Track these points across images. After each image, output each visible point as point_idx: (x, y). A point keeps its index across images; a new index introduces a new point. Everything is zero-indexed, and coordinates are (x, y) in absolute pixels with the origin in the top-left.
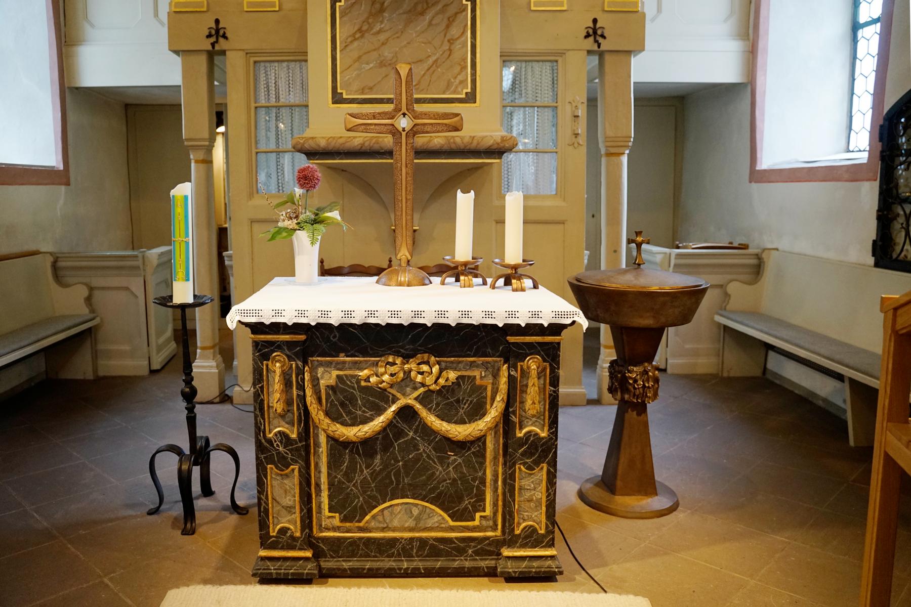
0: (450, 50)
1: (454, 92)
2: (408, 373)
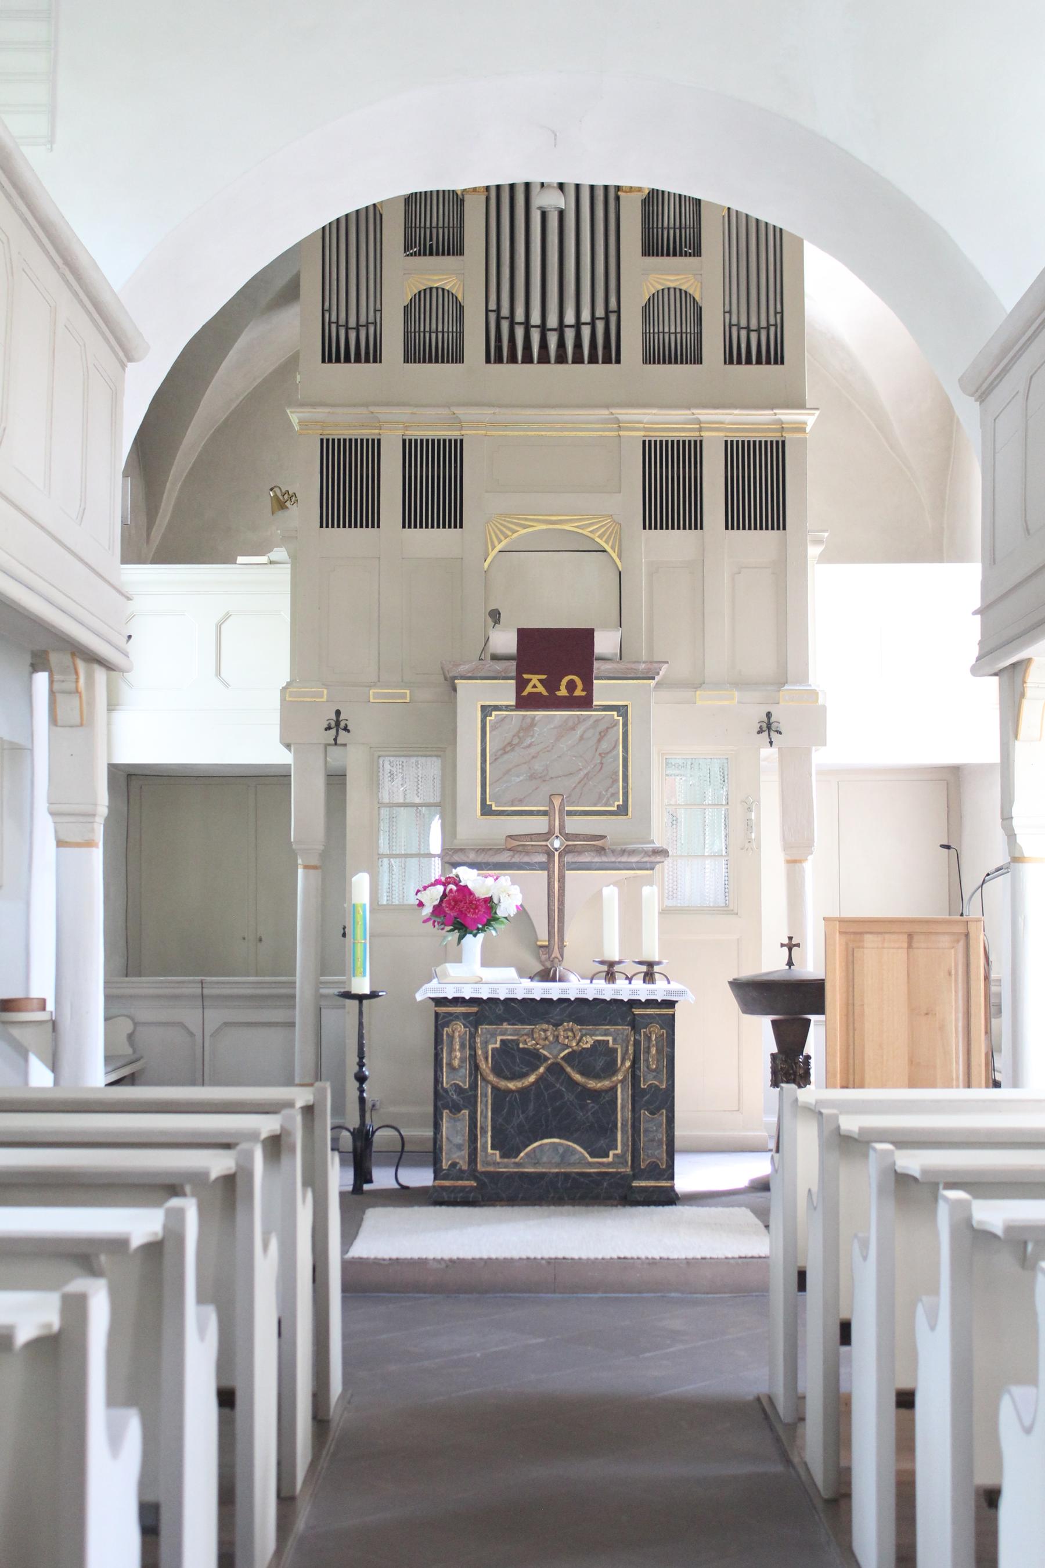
0: (602, 763)
1: (606, 805)
2: (557, 1037)
